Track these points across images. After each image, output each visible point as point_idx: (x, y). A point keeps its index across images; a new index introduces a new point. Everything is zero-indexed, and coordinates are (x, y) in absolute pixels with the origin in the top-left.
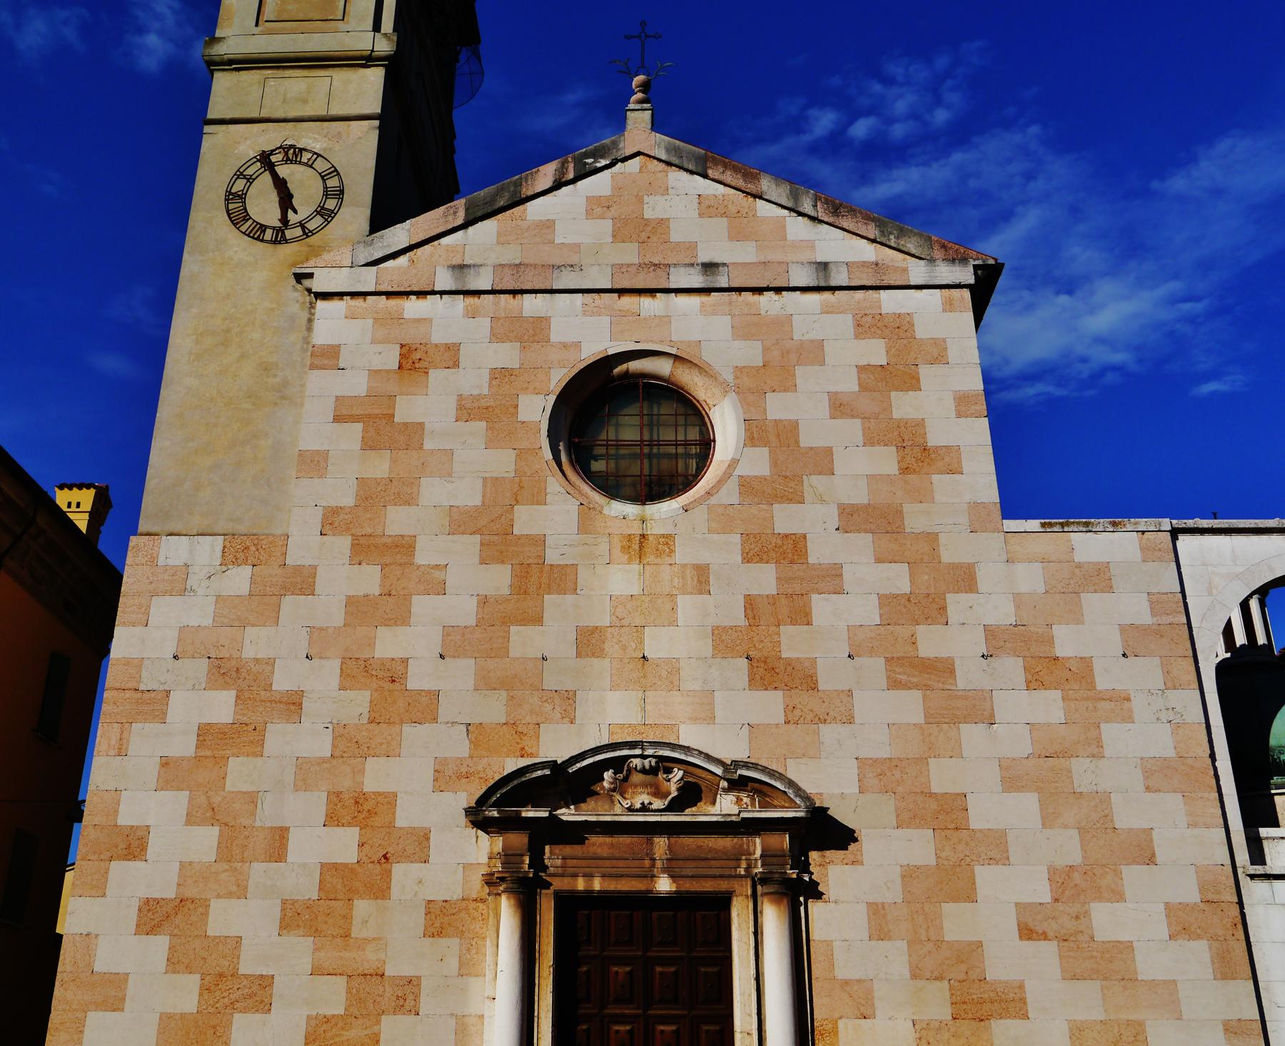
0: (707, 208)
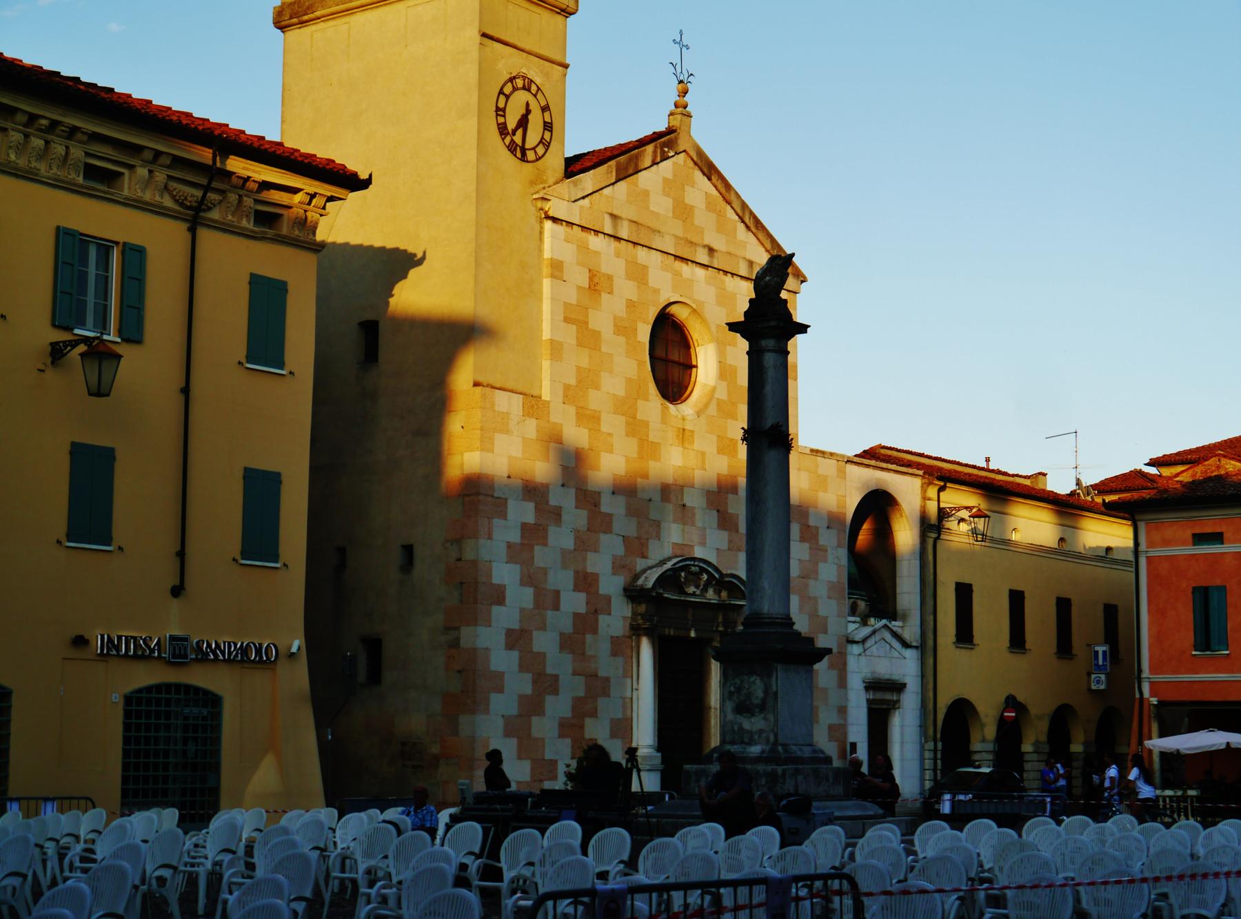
0: (710, 206)
